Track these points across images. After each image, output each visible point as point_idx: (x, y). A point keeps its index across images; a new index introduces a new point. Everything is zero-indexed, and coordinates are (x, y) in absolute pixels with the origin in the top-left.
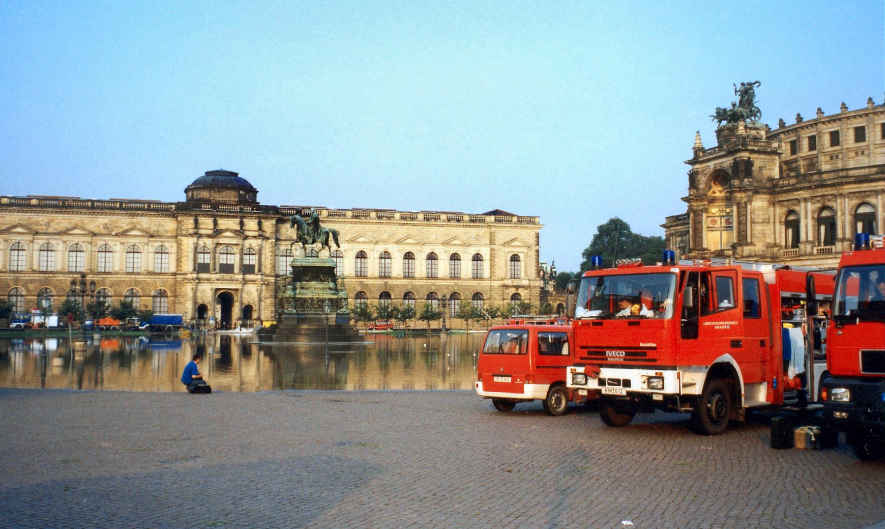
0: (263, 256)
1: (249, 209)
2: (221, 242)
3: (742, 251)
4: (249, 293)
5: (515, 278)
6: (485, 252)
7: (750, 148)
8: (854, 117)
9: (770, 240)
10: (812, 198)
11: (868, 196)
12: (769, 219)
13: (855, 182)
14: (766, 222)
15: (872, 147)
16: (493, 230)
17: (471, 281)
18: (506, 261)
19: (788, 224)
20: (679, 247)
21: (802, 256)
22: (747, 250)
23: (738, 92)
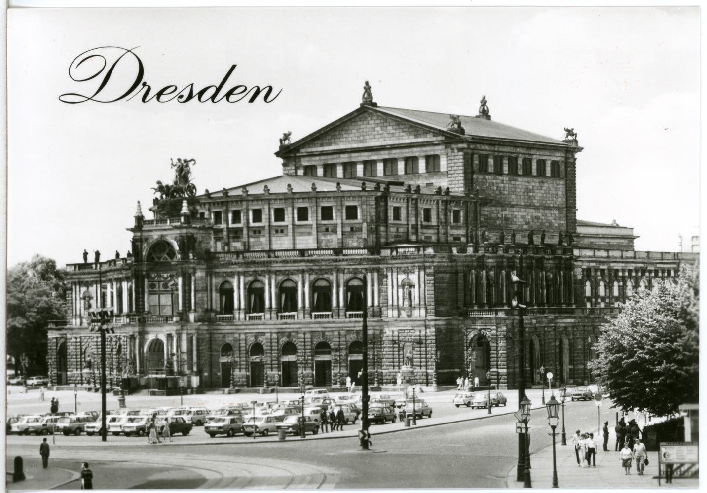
7: (194, 226)
10: (245, 272)
11: (292, 274)
20: (84, 298)
23: (174, 166)
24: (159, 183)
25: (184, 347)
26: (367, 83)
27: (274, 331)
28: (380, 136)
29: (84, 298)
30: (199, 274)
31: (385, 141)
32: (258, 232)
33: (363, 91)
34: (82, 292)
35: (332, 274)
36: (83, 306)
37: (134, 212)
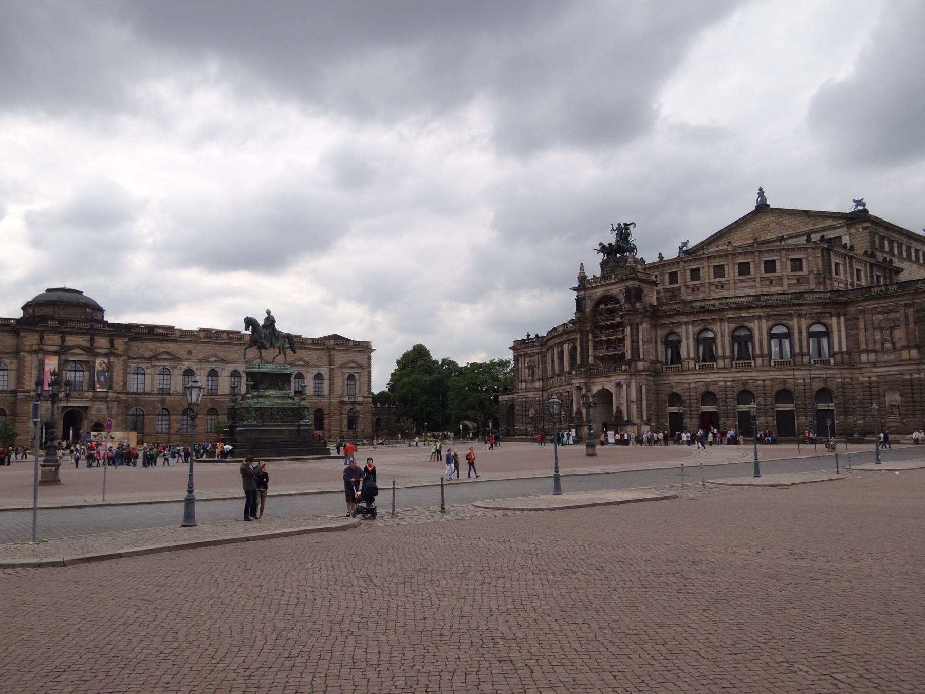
0: (115, 374)
1: (100, 326)
2: (69, 359)
3: (636, 367)
4: (99, 410)
5: (350, 395)
6: (325, 372)
8: (715, 257)
9: (652, 357)
12: (651, 339)
13: (734, 309)
14: (649, 342)
15: (732, 282)
16: (332, 352)
17: (313, 398)
18: (343, 380)
19: (667, 344)
20: (528, 367)
21: (686, 371)
22: (641, 365)
24: (601, 244)
25: (633, 397)
26: (761, 189)
27: (728, 379)
28: (775, 230)
29: (528, 367)
30: (645, 326)
31: (781, 233)
32: (696, 289)
33: (758, 196)
34: (526, 362)
35: (792, 320)
36: (527, 372)
37: (577, 272)
